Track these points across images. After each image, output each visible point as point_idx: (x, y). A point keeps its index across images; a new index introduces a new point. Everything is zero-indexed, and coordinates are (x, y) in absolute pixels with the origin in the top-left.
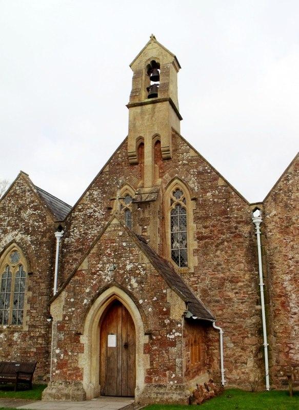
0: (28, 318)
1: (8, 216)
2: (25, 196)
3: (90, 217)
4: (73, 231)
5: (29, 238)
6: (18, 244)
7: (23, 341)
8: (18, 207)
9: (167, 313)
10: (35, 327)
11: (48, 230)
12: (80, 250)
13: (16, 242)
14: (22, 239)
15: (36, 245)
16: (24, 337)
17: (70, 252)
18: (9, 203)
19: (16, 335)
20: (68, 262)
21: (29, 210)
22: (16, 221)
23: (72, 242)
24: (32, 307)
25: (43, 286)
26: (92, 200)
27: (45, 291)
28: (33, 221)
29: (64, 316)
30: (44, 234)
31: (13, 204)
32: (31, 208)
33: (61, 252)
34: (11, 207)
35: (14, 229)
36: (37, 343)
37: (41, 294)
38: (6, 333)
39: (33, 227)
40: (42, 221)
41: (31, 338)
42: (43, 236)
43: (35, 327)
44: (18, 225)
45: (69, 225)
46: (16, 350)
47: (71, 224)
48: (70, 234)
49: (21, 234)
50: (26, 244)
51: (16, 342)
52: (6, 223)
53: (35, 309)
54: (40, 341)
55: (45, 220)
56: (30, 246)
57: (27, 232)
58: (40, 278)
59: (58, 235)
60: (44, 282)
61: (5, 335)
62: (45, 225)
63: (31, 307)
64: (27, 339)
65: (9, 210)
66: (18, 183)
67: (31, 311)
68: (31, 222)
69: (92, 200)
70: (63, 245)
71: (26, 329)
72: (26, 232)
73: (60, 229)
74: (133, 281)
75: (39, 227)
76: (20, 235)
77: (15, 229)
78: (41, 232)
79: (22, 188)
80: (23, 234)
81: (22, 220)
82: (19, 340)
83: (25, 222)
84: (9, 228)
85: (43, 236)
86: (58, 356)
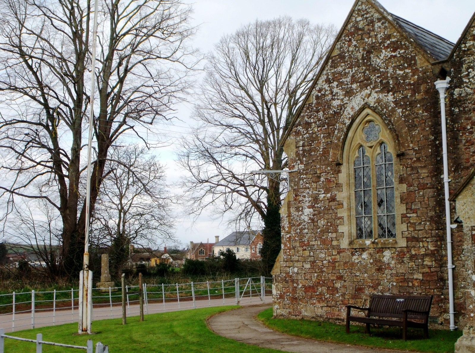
0: (404, 227)
1: (351, 67)
2: (373, 30)
4: (468, 75)
6: (374, 109)
7: (400, 263)
8: (364, 49)
11: (422, 80)
13: (369, 107)
14: (379, 101)
15: (404, 107)
16: (400, 256)
17: (465, 112)
18: (349, 46)
19: (387, 254)
20: (464, 128)
21: (384, 51)
22: (364, 72)
23: (467, 94)
24: (409, 209)
25: (424, 173)
27: (428, 181)
28: (394, 68)
30: (415, 89)
31: (355, 46)
32: (388, 47)
33: (450, 113)
34: (352, 51)
35: (364, 85)
36: (423, 266)
37: (422, 187)
38: (371, 251)
39: (395, 78)
40: (410, 66)
42: (415, 91)
44: (369, 79)
45: (458, 66)
46: (389, 277)
47: (461, 64)
48: (462, 81)
49: (376, 92)
50: (387, 107)
51: (388, 264)
52: (349, 79)
53: (415, 211)
54: (427, 262)
55: (415, 64)
56: (393, 110)
57: (386, 88)
58: (418, 160)
59: (441, 85)
60: (425, 167)
61: (370, 254)
62: (414, 72)
63: (407, 209)
64: (405, 260)
65: (350, 57)
66: (359, 10)
67: (408, 215)
68: (390, 70)
70: (452, 102)
71: (402, 243)
72: (384, 88)
73: (443, 75)
75: (405, 77)
76: (376, 95)
77: (366, 86)
78: (410, 84)
79: (366, 18)
80: (380, 92)
81: (375, 70)
82: (393, 262)
83: (381, 72)
84: (354, 86)
85: (415, 91)
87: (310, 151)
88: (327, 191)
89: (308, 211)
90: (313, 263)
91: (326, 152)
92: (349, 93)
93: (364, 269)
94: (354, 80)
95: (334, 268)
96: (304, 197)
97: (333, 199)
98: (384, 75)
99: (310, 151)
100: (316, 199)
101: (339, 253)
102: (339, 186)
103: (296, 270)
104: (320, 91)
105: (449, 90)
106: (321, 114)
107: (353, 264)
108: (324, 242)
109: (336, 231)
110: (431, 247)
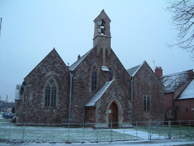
3: (83, 71)
4: (77, 75)
5: (58, 75)
6: (54, 77)
9: (128, 106)
10: (62, 107)
12: (78, 82)
13: (53, 76)
24: (61, 101)
26: (84, 66)
29: (101, 106)
30: (65, 75)
32: (59, 63)
33: (72, 82)
35: (52, 70)
41: (60, 111)
43: (62, 107)
53: (62, 101)
54: (64, 112)
57: (57, 72)
58: (64, 90)
59: (71, 76)
60: (65, 92)
62: (65, 71)
69: (84, 66)
70: (73, 80)
74: (120, 97)
81: (55, 67)
84: (49, 69)
86: (99, 117)
87: (34, 82)
88: (38, 93)
89: (31, 98)
90: (32, 112)
91: (39, 84)
92: (47, 71)
93: (48, 113)
94: (49, 68)
95: (39, 113)
96: (31, 94)
97: (40, 96)
98: (57, 69)
99: (34, 82)
100: (34, 95)
101: (40, 109)
102: (42, 92)
103: (26, 113)
104: (39, 68)
105: (73, 77)
106: (38, 74)
107: (45, 112)
108: (36, 106)
109: (40, 103)
110: (65, 109)
